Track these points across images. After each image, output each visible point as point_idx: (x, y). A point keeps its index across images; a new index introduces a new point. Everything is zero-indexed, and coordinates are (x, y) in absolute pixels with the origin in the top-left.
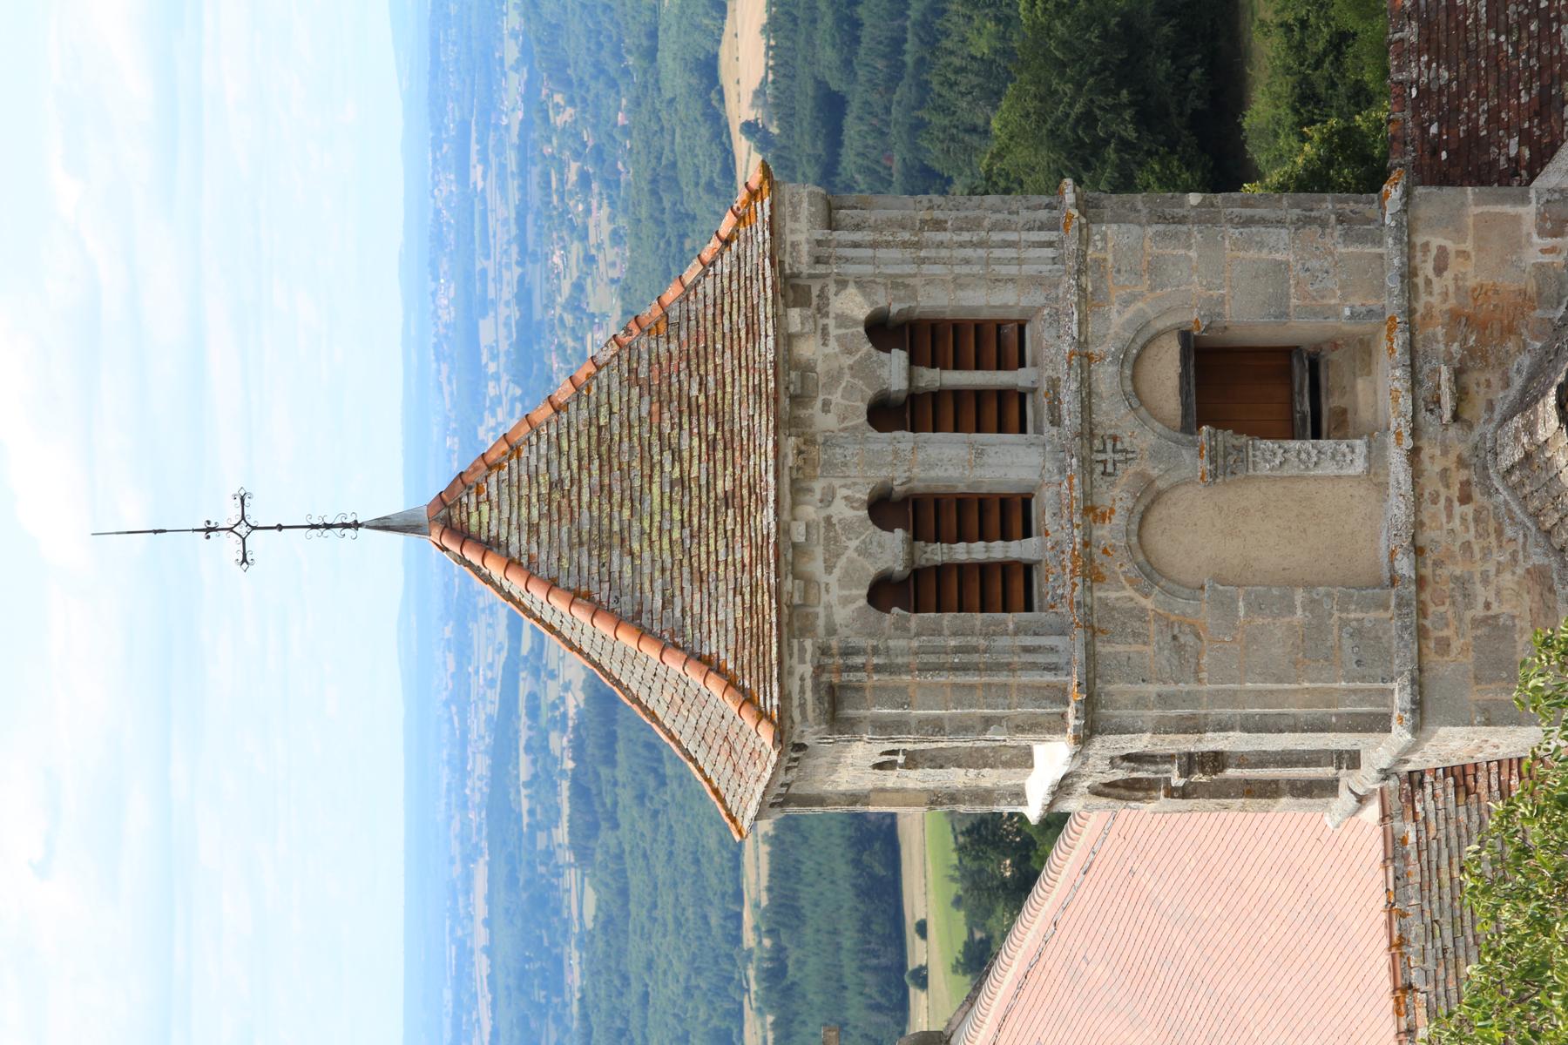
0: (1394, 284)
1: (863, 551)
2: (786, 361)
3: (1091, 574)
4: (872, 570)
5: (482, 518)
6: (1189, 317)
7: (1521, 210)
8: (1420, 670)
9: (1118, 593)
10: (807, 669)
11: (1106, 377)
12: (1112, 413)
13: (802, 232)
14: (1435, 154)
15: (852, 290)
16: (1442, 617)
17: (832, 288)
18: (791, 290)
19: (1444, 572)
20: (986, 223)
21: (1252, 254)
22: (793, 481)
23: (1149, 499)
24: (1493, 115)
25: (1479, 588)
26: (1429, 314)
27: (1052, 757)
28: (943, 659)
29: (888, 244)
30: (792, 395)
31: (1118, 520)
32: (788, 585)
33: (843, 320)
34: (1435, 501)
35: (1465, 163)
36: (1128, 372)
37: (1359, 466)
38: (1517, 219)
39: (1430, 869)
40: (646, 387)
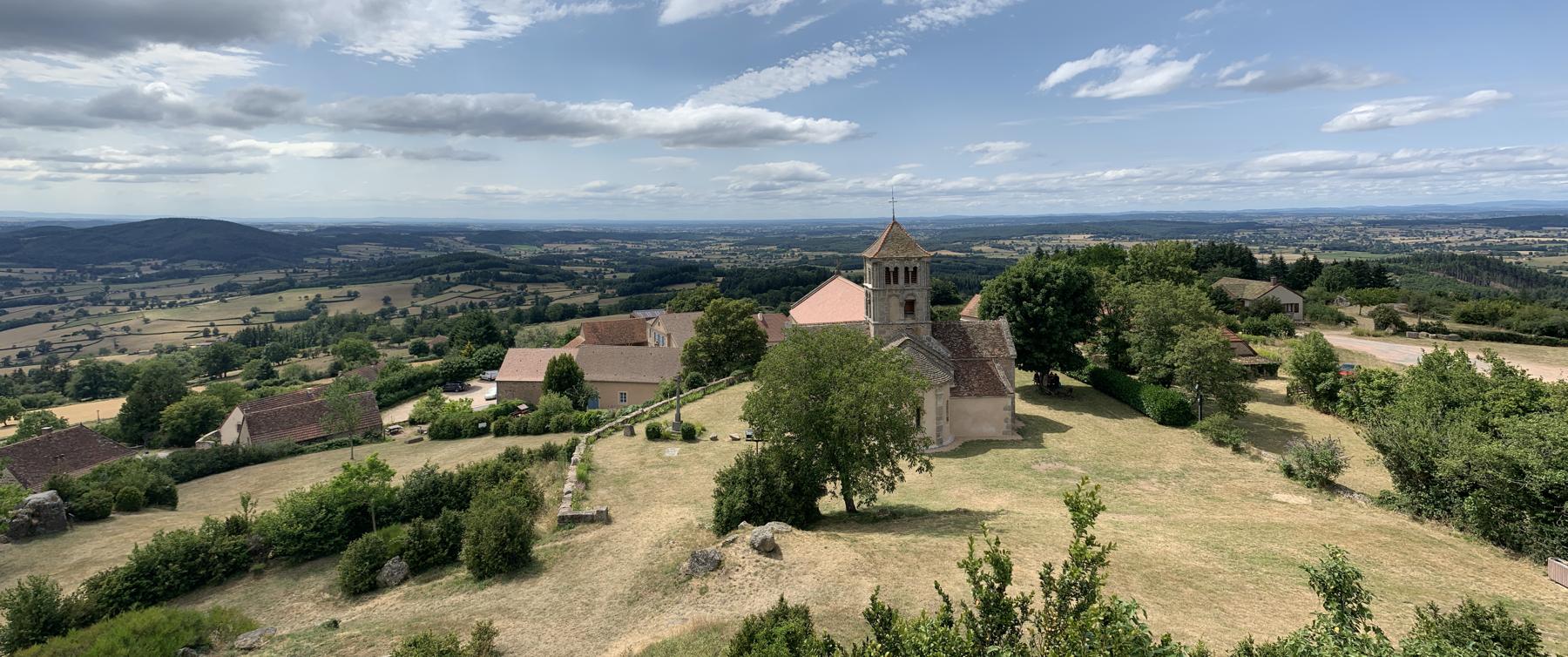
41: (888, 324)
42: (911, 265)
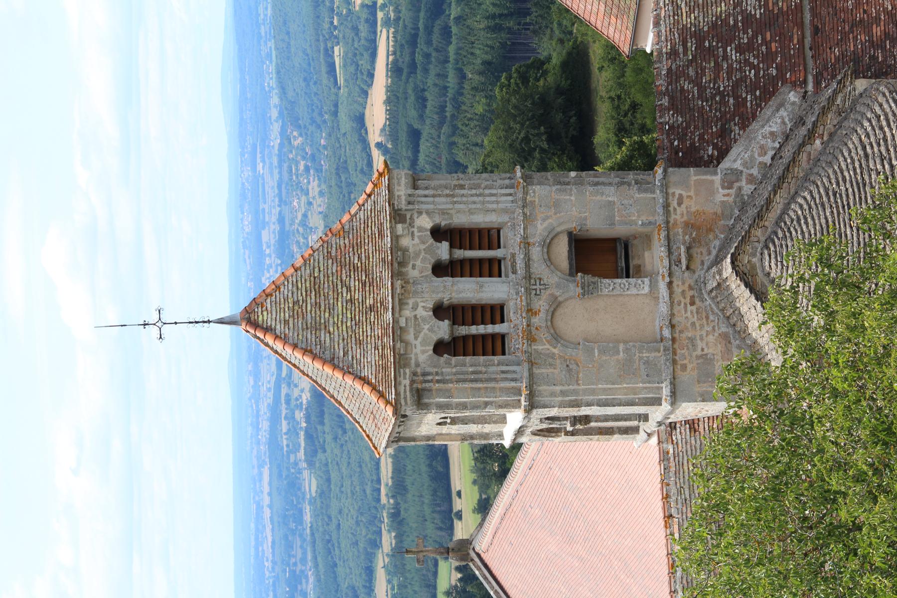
0: (660, 210)
1: (431, 330)
2: (396, 247)
3: (531, 339)
4: (435, 338)
5: (264, 317)
6: (572, 225)
7: (714, 178)
8: (674, 378)
9: (543, 347)
10: (407, 382)
11: (536, 252)
12: (539, 268)
13: (402, 191)
14: (677, 153)
15: (424, 216)
16: (683, 355)
17: (416, 215)
18: (398, 216)
19: (684, 335)
20: (483, 186)
21: (599, 198)
22: (400, 300)
23: (555, 305)
24: (701, 137)
25: (699, 342)
26: (675, 223)
27: (515, 418)
28: (466, 377)
29: (440, 196)
30: (399, 262)
31: (542, 315)
32: (398, 345)
33: (421, 229)
34: (679, 305)
35: (689, 158)
36: (545, 250)
37: (647, 290)
38: (712, 182)
39: (679, 465)
40: (335, 260)
41: (671, 343)
42: (424, 251)
